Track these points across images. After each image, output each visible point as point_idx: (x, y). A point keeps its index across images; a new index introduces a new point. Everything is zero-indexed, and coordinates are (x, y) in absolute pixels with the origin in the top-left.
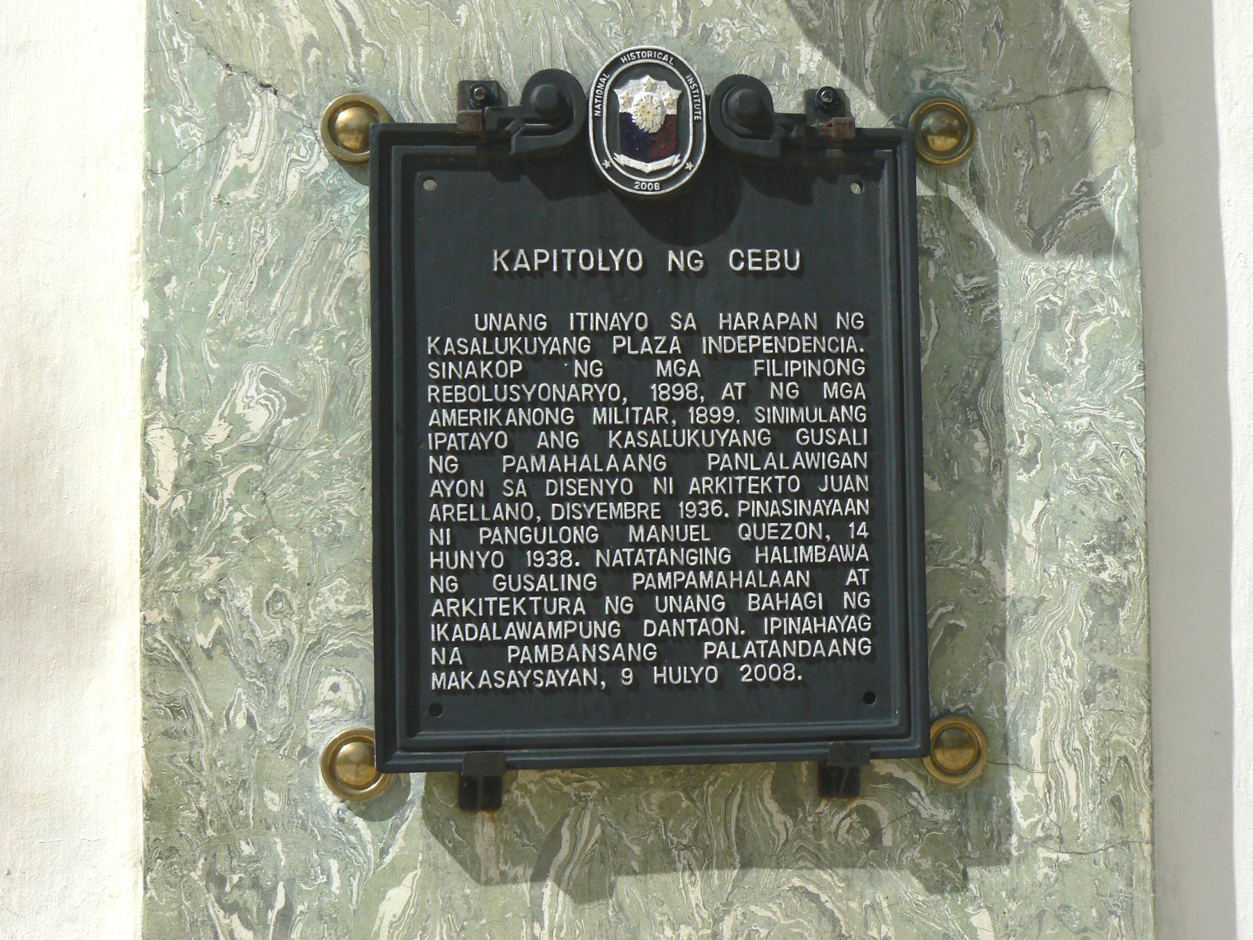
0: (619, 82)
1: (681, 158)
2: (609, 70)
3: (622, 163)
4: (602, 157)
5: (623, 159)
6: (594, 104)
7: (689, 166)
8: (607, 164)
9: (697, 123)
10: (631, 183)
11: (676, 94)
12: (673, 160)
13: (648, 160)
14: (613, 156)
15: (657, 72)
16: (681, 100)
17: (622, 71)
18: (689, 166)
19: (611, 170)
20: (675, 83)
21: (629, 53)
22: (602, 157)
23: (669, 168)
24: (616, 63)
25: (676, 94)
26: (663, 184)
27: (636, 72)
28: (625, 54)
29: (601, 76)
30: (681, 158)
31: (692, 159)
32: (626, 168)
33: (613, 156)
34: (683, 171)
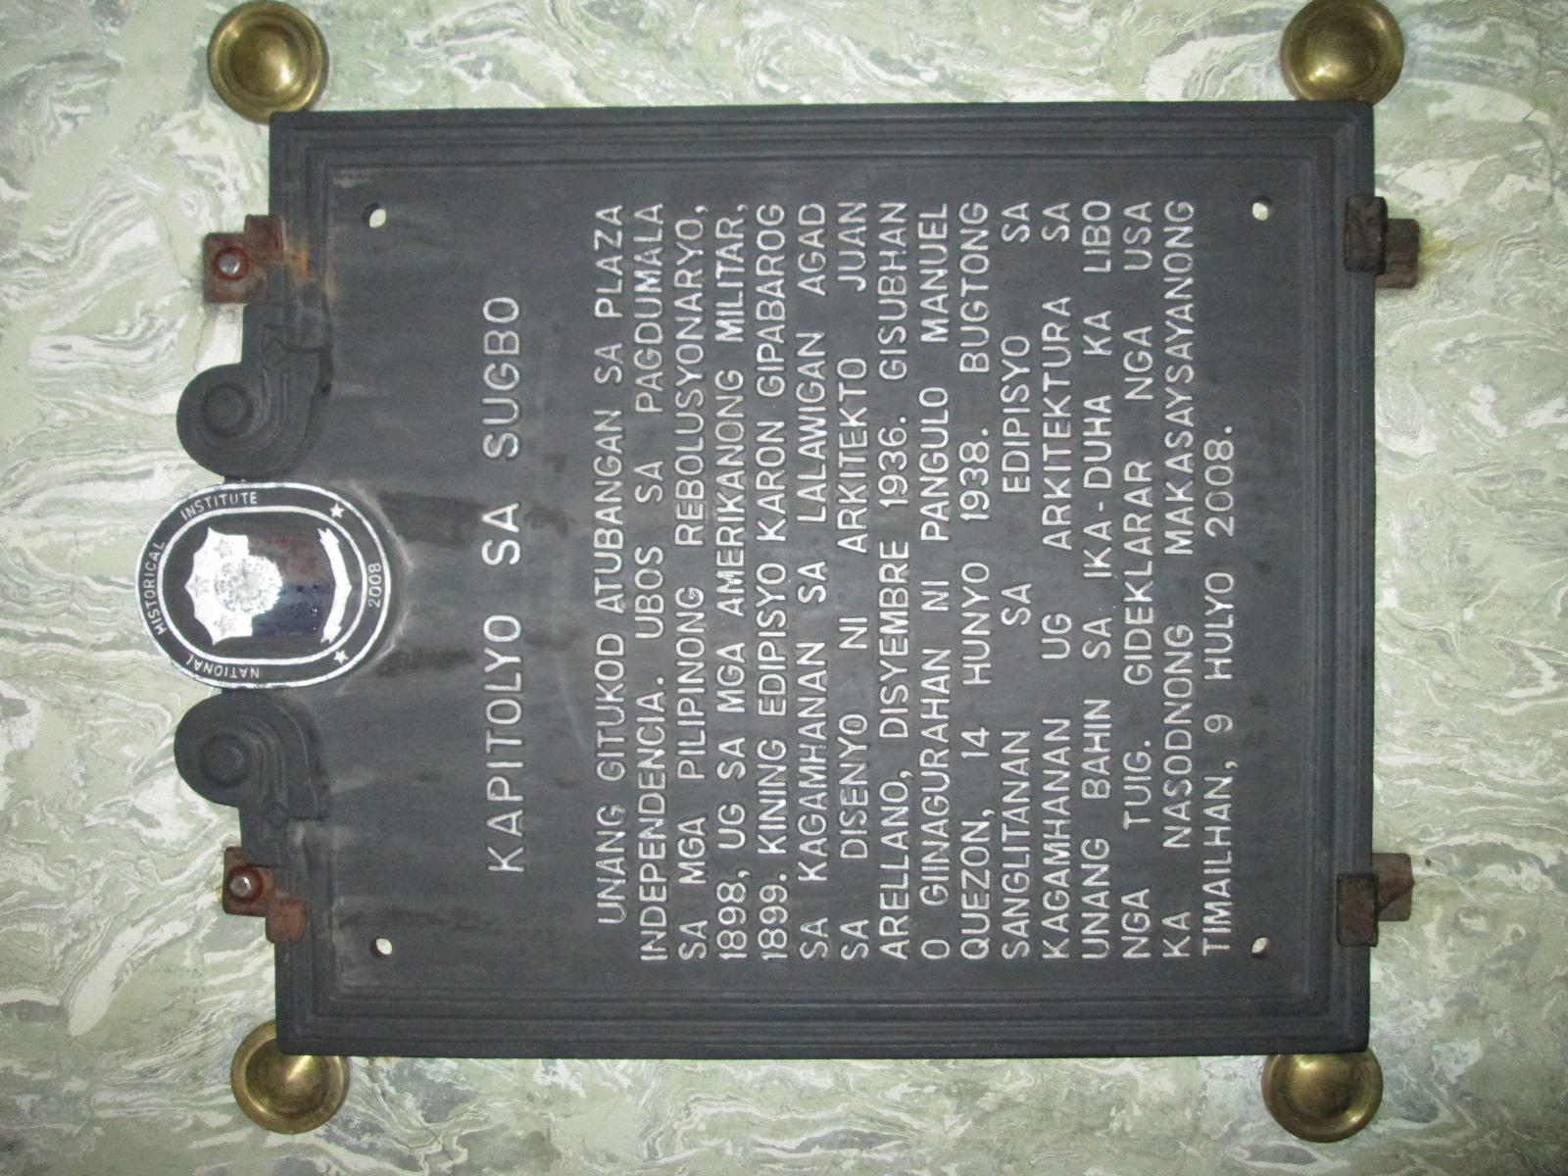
0: (199, 635)
1: (325, 526)
2: (179, 654)
3: (338, 630)
4: (329, 664)
5: (331, 629)
6: (240, 679)
7: (337, 511)
8: (341, 657)
9: (265, 497)
10: (372, 614)
11: (213, 537)
12: (329, 541)
13: (327, 588)
14: (327, 645)
15: (180, 567)
16: (225, 525)
17: (180, 630)
18: (337, 511)
19: (351, 648)
20: (196, 538)
21: (149, 621)
22: (329, 664)
23: (345, 547)
24: (167, 641)
25: (213, 537)
26: (371, 557)
27: (182, 607)
28: (152, 627)
29: (191, 668)
30: (325, 526)
31: (325, 505)
32: (345, 624)
33: (327, 645)
34: (348, 520)
